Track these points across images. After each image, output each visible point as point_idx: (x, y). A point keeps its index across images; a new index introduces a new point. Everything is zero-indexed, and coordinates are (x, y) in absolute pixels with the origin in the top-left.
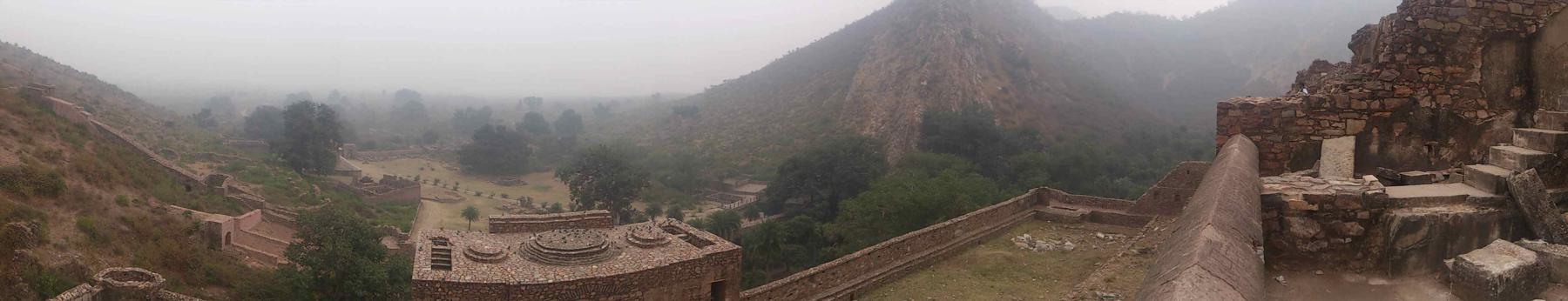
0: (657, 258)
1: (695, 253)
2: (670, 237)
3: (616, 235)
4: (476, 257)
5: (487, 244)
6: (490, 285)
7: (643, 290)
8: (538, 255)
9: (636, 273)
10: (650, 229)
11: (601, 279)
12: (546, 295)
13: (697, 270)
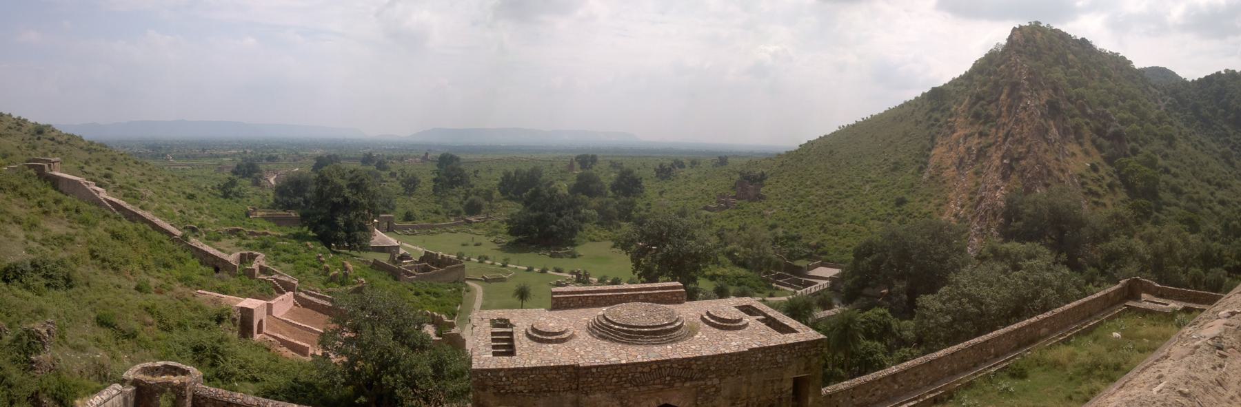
0: (733, 343)
1: (777, 339)
2: (747, 319)
3: (689, 311)
4: (539, 336)
5: (550, 320)
6: (557, 368)
7: (721, 378)
8: (605, 331)
9: (713, 357)
10: (727, 307)
11: (677, 360)
12: (620, 378)
13: (779, 358)
